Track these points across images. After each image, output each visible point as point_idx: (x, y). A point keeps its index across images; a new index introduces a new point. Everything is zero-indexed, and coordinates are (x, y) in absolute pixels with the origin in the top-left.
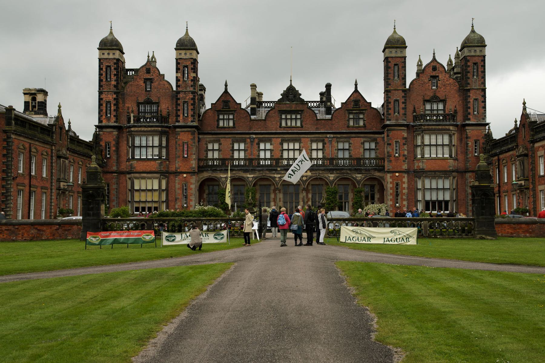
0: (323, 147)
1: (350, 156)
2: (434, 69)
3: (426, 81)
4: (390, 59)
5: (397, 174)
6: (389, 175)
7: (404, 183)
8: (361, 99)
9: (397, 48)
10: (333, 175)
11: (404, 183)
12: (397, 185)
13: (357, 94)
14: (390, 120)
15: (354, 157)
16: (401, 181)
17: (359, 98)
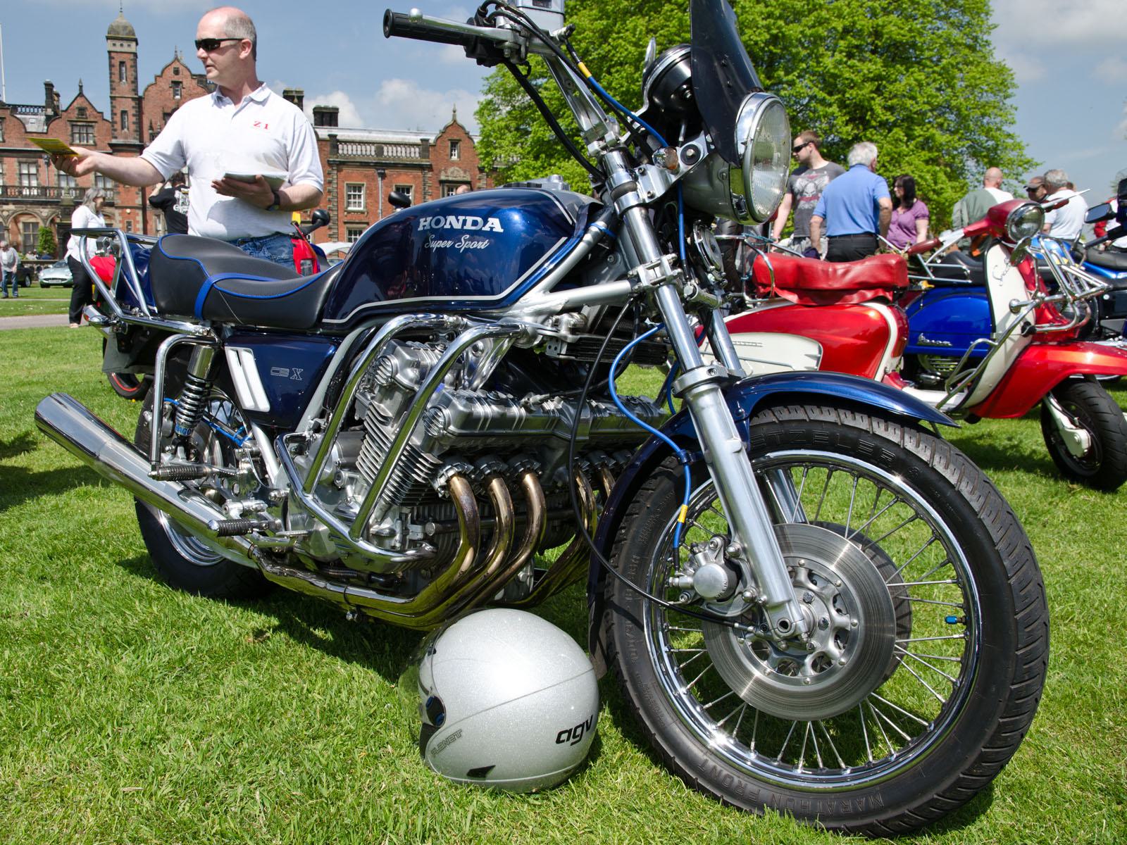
0: (37, 170)
1: (77, 185)
2: (177, 72)
3: (166, 87)
4: (113, 55)
5: (128, 211)
6: (117, 212)
7: (138, 222)
8: (89, 107)
9: (122, 39)
10: (46, 210)
11: (138, 222)
12: (129, 223)
13: (83, 99)
14: (116, 138)
15: (80, 186)
16: (134, 219)
17: (85, 105)
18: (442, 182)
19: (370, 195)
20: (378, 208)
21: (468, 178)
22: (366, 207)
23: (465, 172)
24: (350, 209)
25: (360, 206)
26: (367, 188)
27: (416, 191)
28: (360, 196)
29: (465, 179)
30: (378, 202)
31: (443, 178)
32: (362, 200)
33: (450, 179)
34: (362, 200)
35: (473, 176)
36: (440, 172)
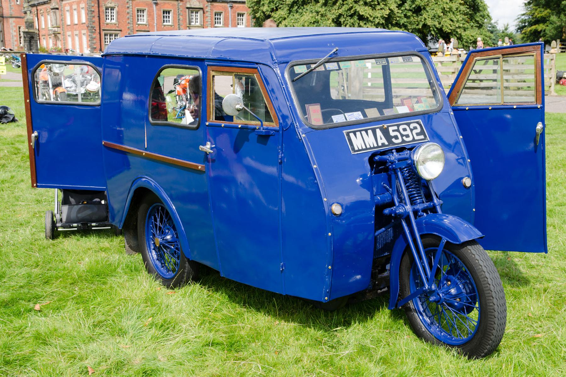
18: (187, 8)
19: (150, 15)
20: (154, 23)
21: (202, 6)
22: (148, 21)
23: (199, 2)
24: (139, 23)
25: (144, 21)
26: (148, 11)
27: (174, 13)
28: (143, 16)
29: (200, 7)
30: (153, 19)
31: (188, 6)
32: (145, 18)
33: (192, 6)
34: (145, 18)
35: (204, 5)
36: (186, 2)
